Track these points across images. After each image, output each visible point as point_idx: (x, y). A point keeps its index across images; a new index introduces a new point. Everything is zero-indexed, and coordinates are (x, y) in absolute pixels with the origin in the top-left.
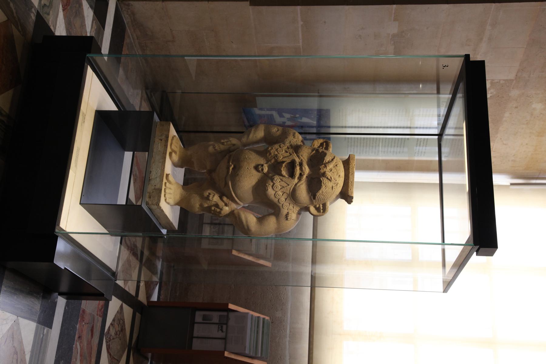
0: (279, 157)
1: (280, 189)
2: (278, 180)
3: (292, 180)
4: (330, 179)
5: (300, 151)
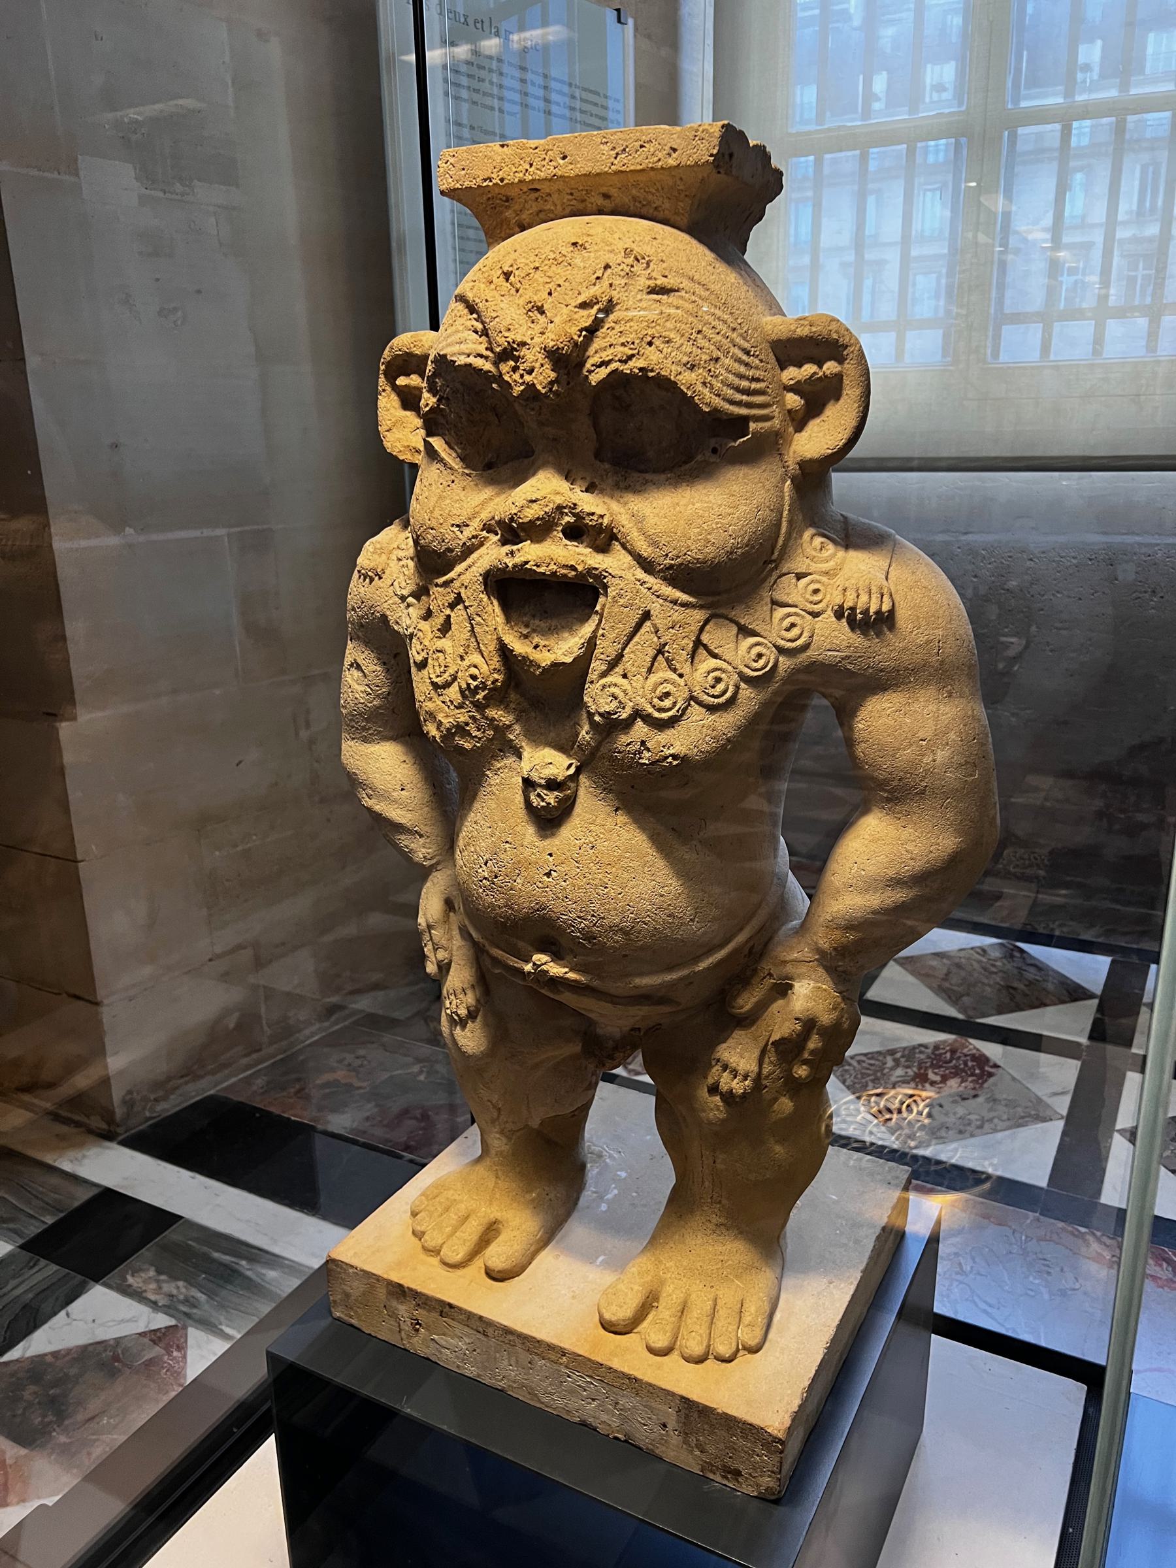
0: (474, 678)
1: (675, 670)
2: (613, 690)
3: (612, 592)
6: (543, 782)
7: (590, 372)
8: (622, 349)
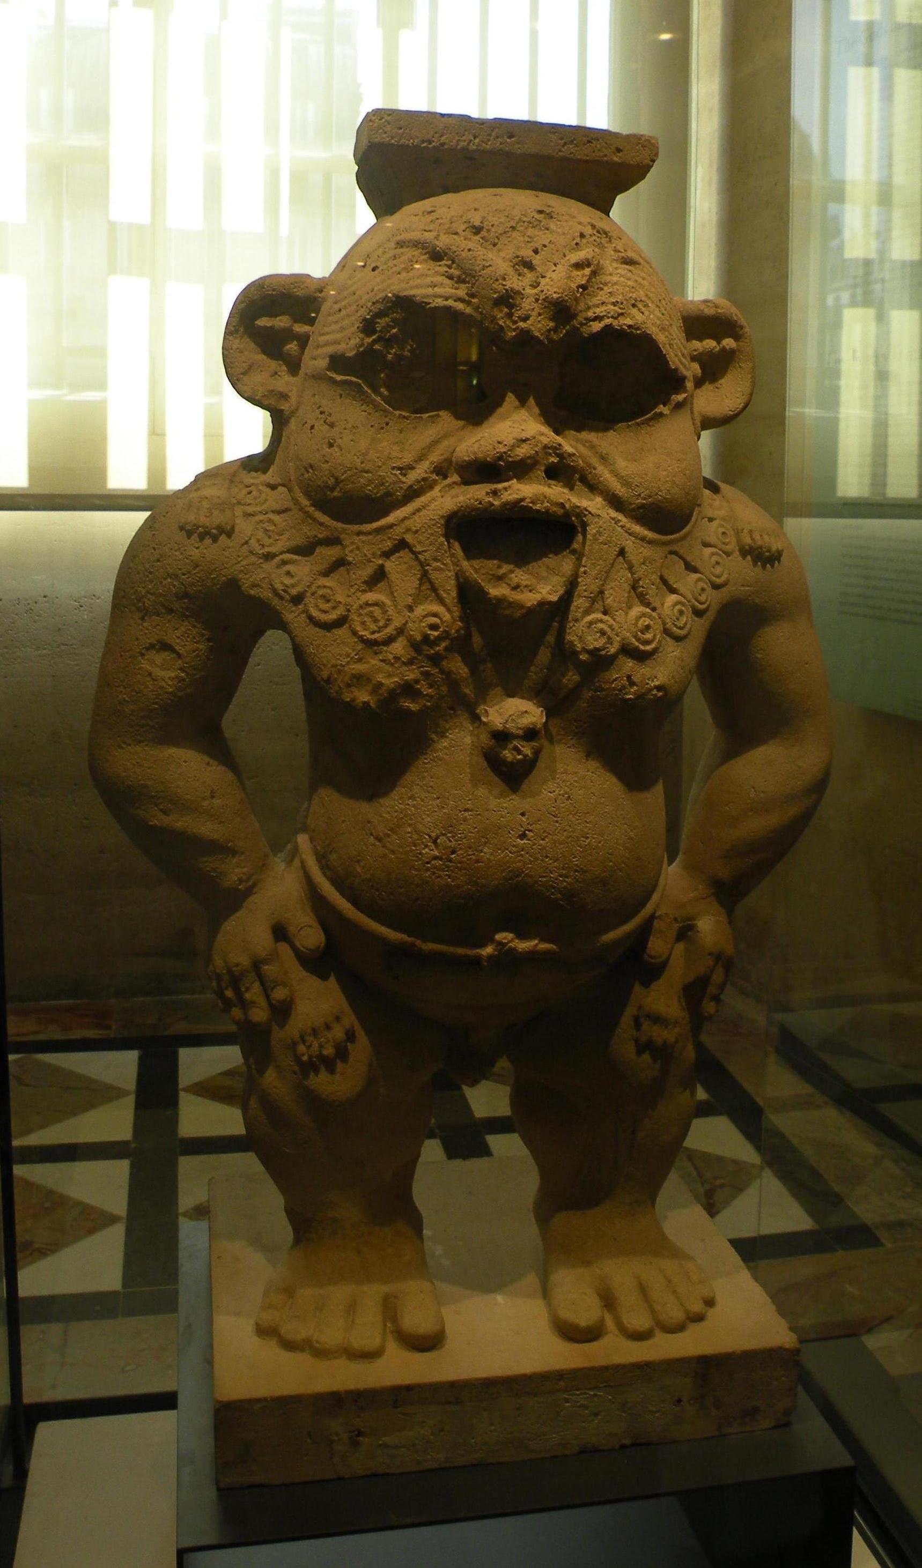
0: (433, 627)
1: (647, 605)
2: (600, 625)
3: (591, 530)
4: (587, 271)
5: (370, 482)
6: (520, 732)
7: (582, 324)
8: (612, 307)
